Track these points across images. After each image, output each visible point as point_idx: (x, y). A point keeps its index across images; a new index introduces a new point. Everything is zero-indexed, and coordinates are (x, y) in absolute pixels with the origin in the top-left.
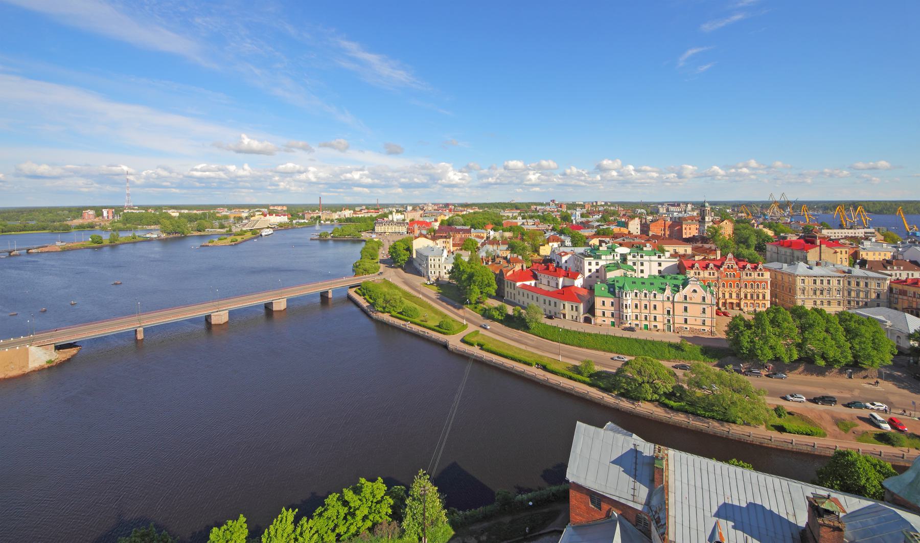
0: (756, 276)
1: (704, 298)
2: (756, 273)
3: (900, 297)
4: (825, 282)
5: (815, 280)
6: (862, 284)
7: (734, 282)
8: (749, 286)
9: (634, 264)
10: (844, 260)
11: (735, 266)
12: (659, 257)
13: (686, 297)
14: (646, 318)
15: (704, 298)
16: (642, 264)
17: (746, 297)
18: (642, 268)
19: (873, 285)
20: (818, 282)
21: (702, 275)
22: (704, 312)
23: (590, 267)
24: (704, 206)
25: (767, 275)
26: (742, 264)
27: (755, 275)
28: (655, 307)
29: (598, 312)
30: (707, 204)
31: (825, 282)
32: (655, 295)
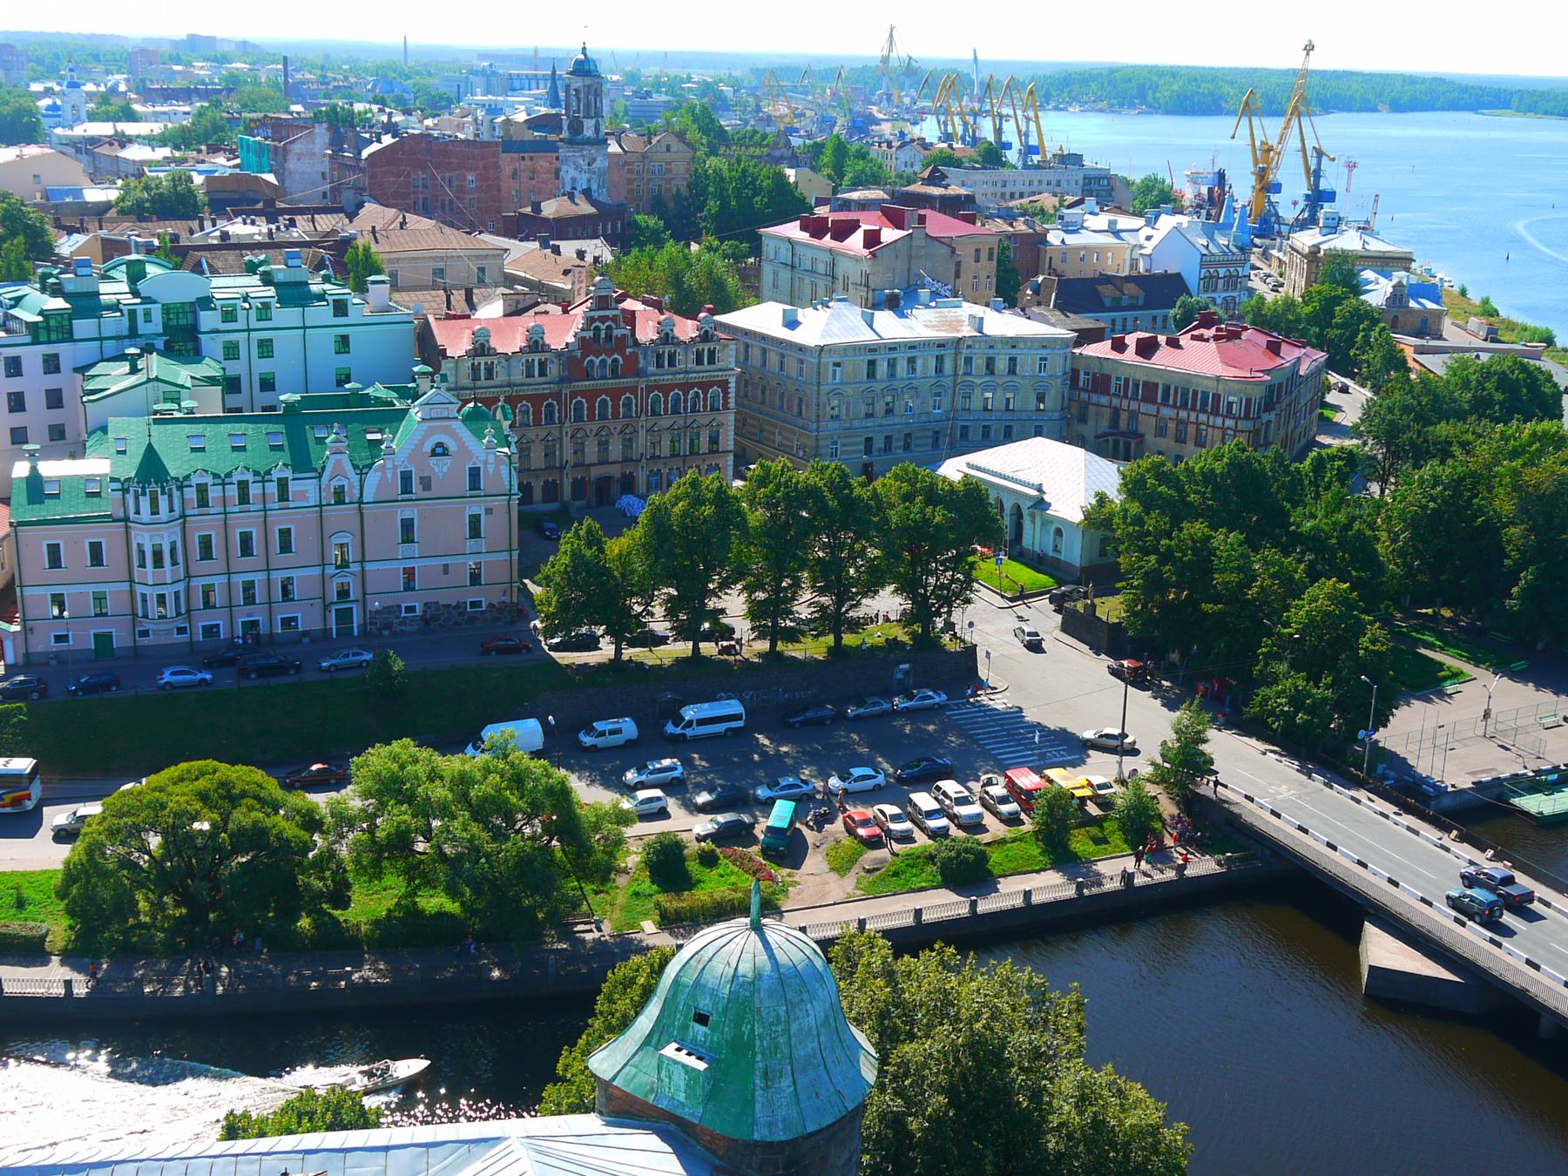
0: (692, 365)
1: (475, 474)
3: (1095, 398)
4: (902, 367)
5: (872, 364)
6: (1002, 365)
9: (231, 352)
10: (983, 275)
12: (340, 308)
13: (406, 478)
14: (250, 599)
15: (475, 474)
16: (266, 348)
18: (262, 366)
19: (1027, 365)
20: (882, 369)
22: (475, 532)
23: (15, 384)
28: (285, 534)
31: (902, 367)
32: (283, 484)
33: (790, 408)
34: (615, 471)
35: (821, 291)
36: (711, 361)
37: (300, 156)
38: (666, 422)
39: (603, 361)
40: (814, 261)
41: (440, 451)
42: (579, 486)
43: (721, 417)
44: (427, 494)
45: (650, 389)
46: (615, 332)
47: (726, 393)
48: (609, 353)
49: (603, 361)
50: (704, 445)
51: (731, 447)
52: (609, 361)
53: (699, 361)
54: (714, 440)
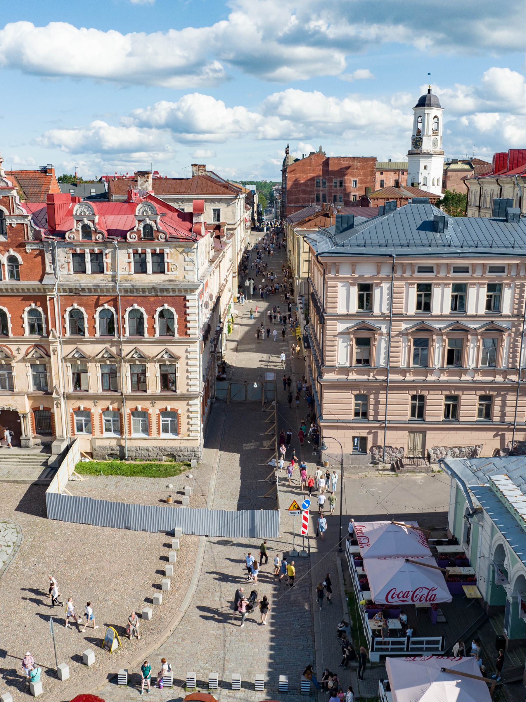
43: (177, 350)
53: (141, 268)
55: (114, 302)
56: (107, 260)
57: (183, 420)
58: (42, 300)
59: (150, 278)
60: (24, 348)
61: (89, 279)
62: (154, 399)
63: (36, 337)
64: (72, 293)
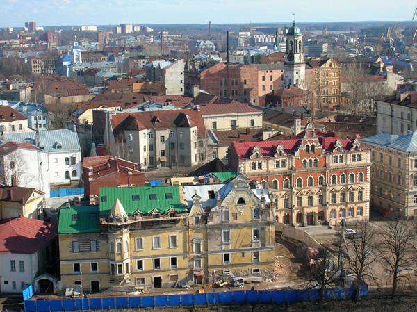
0: (350, 162)
2: (350, 156)
7: (304, 174)
8: (339, 178)
11: (318, 147)
17: (334, 200)
21: (264, 169)
24: (292, 33)
25: (366, 158)
26: (328, 140)
27: (349, 160)
29: (66, 265)
30: (297, 30)
33: (395, 181)
34: (316, 210)
35: (406, 127)
36: (359, 159)
37: (171, 74)
38: (338, 188)
39: (310, 160)
40: (402, 113)
41: (241, 201)
42: (300, 217)
44: (235, 221)
45: (331, 172)
46: (316, 148)
47: (366, 174)
48: (313, 157)
49: (310, 160)
50: (356, 199)
51: (368, 199)
52: (313, 160)
54: (361, 193)
55: (346, 172)
56: (344, 158)
57: (364, 210)
58: (324, 173)
59: (357, 162)
60: (317, 190)
61: (339, 164)
62: (356, 203)
63: (321, 186)
64: (334, 170)
